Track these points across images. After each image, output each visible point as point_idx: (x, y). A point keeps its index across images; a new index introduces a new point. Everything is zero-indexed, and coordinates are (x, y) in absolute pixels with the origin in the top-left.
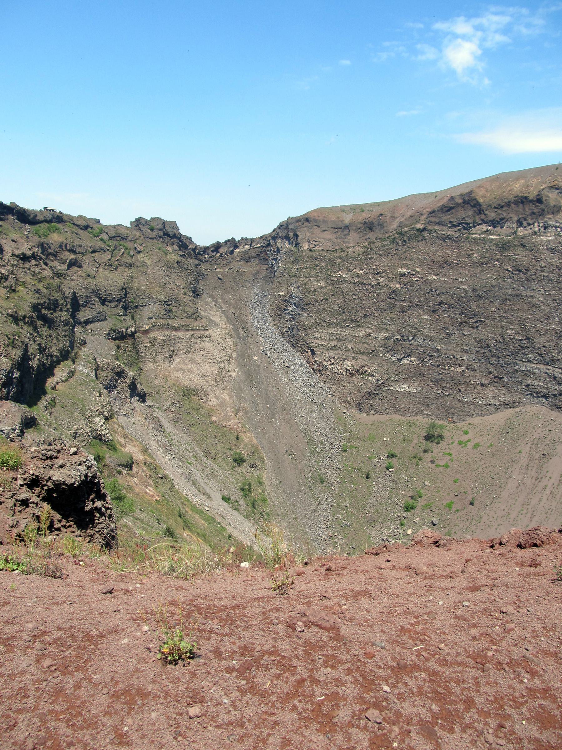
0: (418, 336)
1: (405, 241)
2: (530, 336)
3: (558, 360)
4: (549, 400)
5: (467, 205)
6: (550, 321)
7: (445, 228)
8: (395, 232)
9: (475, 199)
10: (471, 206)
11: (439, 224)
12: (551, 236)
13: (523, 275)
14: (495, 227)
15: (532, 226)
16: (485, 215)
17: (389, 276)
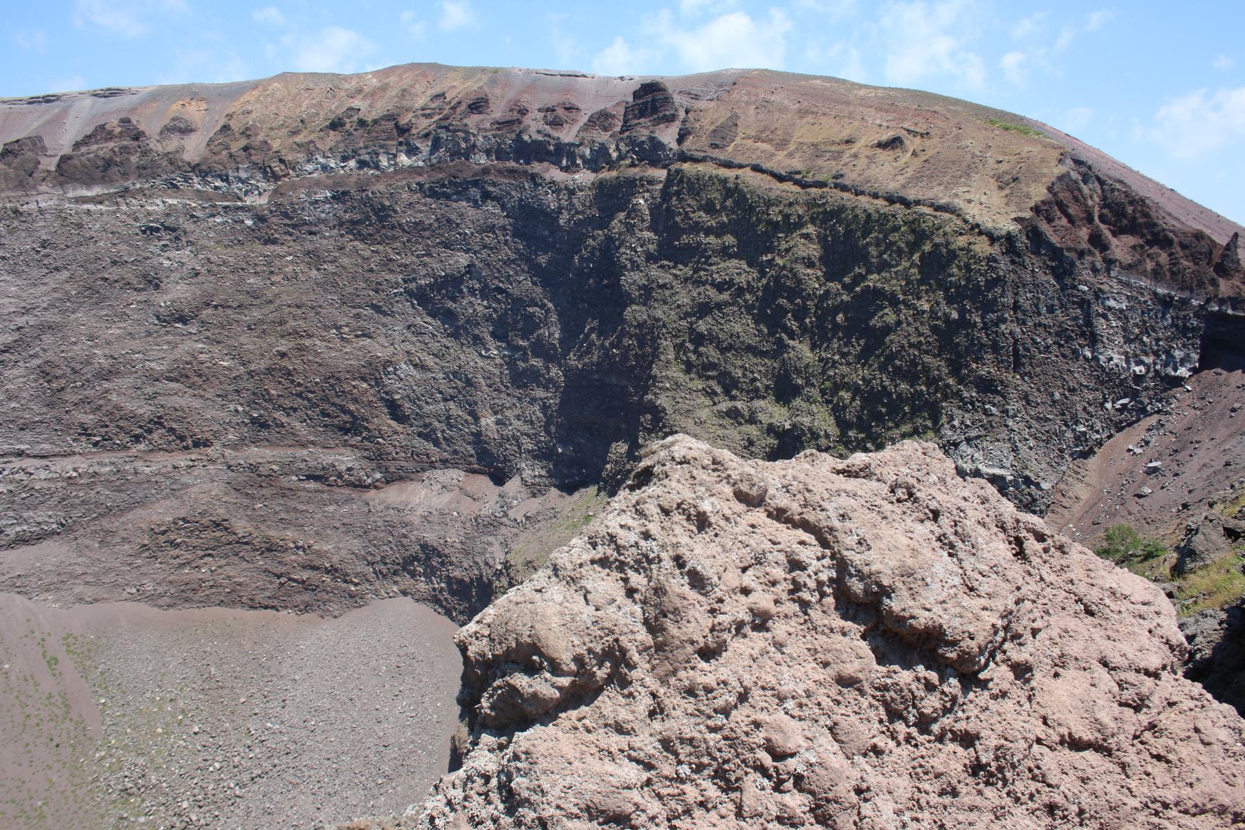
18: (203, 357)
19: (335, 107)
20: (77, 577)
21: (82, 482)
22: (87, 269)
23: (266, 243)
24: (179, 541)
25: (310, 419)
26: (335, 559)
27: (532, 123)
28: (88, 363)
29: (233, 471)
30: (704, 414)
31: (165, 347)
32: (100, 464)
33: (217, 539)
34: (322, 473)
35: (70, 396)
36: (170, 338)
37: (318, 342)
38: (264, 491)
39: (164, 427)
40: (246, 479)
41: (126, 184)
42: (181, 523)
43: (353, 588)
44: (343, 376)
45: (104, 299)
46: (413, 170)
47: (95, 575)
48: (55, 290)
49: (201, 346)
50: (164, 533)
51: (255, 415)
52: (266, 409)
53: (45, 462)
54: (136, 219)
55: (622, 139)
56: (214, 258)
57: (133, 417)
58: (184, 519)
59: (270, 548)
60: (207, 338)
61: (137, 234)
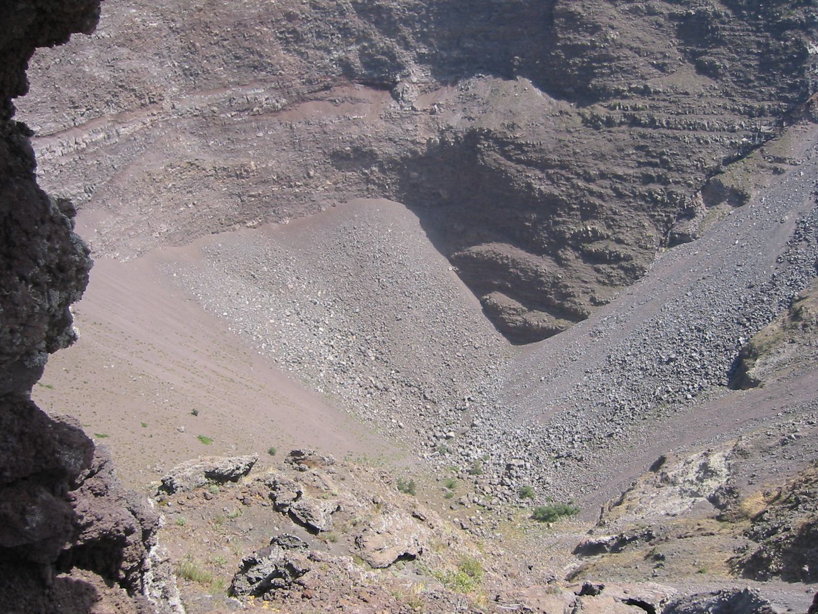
18: (138, 20)
21: (91, 150)
24: (170, 185)
25: (226, 63)
30: (614, 12)
32: (96, 132)
34: (247, 106)
38: (213, 130)
39: (126, 89)
42: (170, 169)
43: (297, 190)
47: (131, 229)
49: (134, 11)
50: (161, 181)
51: (187, 67)
52: (194, 60)
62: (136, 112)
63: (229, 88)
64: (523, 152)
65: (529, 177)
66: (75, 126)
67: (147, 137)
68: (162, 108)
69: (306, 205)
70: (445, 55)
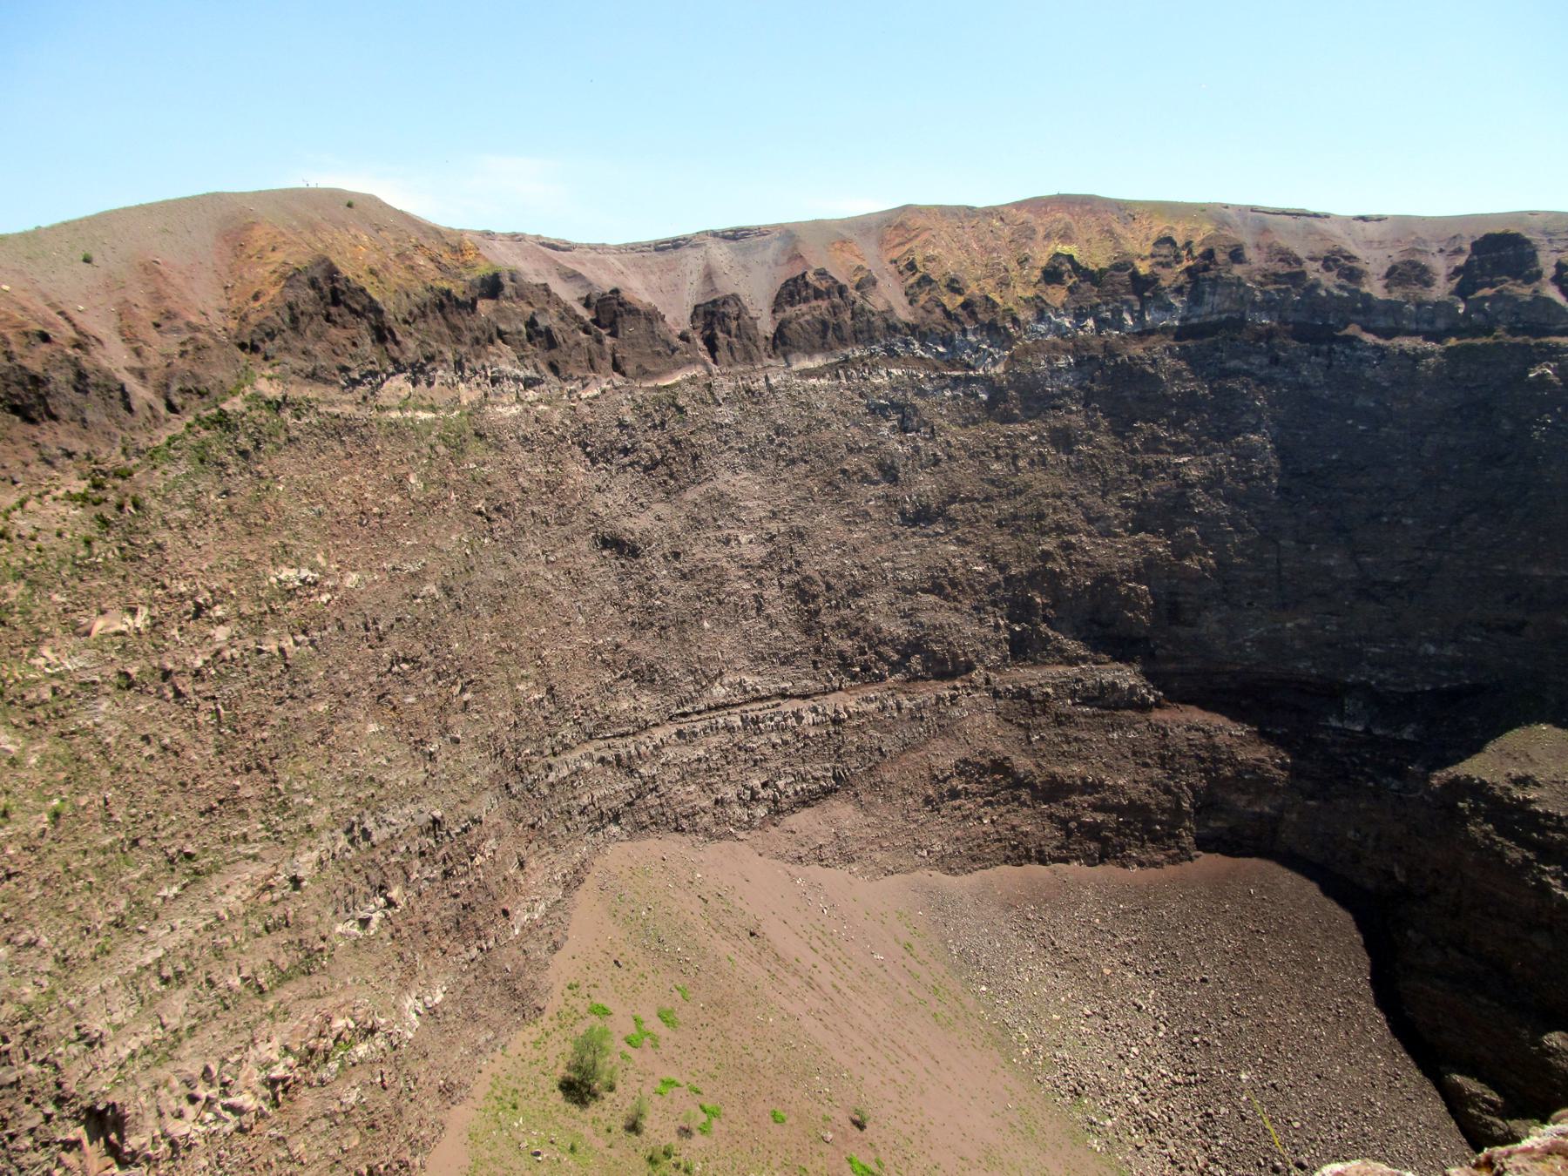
0: (383, 804)
1: (244, 454)
2: (552, 682)
3: (607, 718)
4: (623, 821)
5: (333, 310)
6: (573, 627)
7: (333, 393)
8: (190, 419)
9: (363, 290)
10: (353, 311)
11: (313, 376)
12: (513, 404)
13: (504, 520)
14: (414, 384)
15: (477, 377)
16: (397, 343)
17: (246, 609)
18: (957, 562)
19: (1042, 255)
20: (872, 843)
21: (854, 724)
22: (826, 460)
23: (1002, 423)
24: (960, 787)
26: (1134, 795)
27: (1317, 275)
28: (842, 576)
29: (1001, 698)
31: (914, 552)
32: (868, 700)
33: (995, 782)
35: (827, 619)
36: (917, 540)
37: (1084, 538)
38: (1043, 720)
40: (1018, 706)
41: (845, 352)
44: (1117, 576)
45: (844, 495)
46: (1165, 330)
47: (885, 837)
48: (797, 487)
49: (953, 548)
50: (945, 780)
53: (810, 703)
54: (861, 395)
55: (1484, 298)
56: (953, 441)
57: (893, 642)
58: (965, 762)
59: (1055, 790)
60: (958, 538)
61: (866, 414)
62: (932, 682)
63: (1077, 665)
64: (1542, 830)
65: (1544, 872)
66: (840, 689)
67: (942, 716)
68: (971, 681)
69: (1170, 852)
70: (1432, 649)
